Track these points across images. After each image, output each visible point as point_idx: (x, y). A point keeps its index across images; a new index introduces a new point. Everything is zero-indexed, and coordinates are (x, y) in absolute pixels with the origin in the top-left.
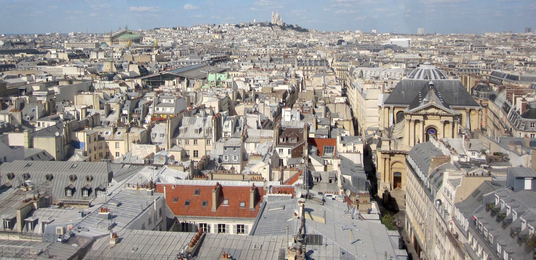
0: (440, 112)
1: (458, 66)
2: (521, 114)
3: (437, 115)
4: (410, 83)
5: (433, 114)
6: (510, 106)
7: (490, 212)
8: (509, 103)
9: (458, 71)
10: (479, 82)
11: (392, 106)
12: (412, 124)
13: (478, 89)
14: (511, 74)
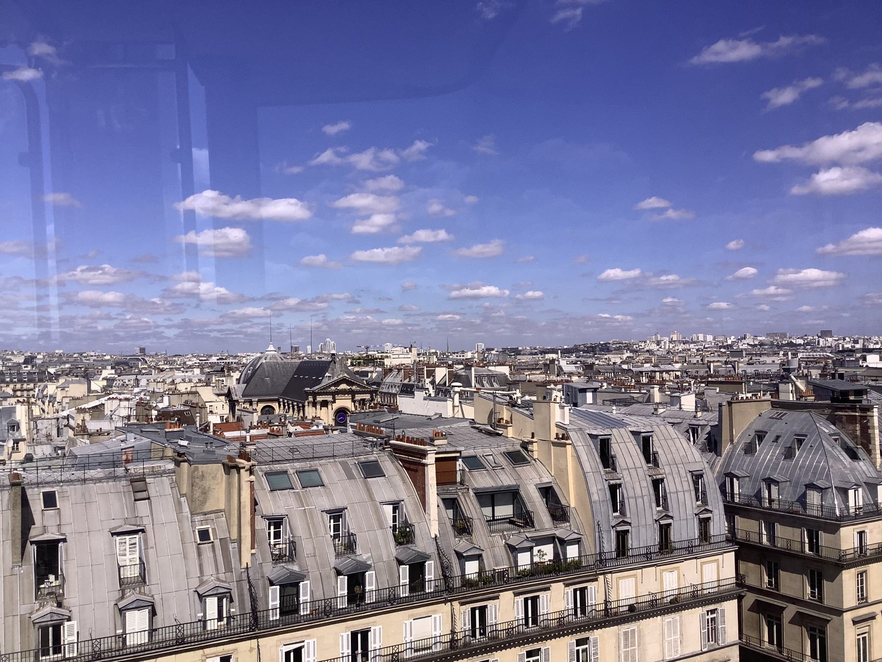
0: (354, 388)
4: (276, 366)
5: (344, 392)
11: (255, 399)
12: (318, 407)
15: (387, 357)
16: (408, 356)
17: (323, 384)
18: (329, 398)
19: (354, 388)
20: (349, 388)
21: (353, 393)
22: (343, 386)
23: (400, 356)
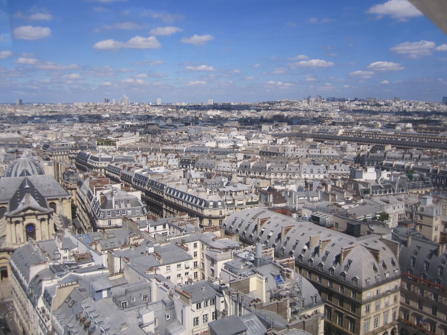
0: (37, 212)
1: (52, 146)
2: (100, 205)
3: (34, 214)
5: (30, 214)
6: (93, 195)
7: (79, 322)
8: (92, 193)
9: (52, 150)
10: (69, 169)
12: (13, 225)
13: (68, 174)
14: (93, 156)
15: (118, 140)
16: (133, 138)
17: (16, 211)
18: (20, 219)
19: (37, 212)
20: (33, 212)
21: (37, 215)
22: (29, 211)
23: (128, 138)
